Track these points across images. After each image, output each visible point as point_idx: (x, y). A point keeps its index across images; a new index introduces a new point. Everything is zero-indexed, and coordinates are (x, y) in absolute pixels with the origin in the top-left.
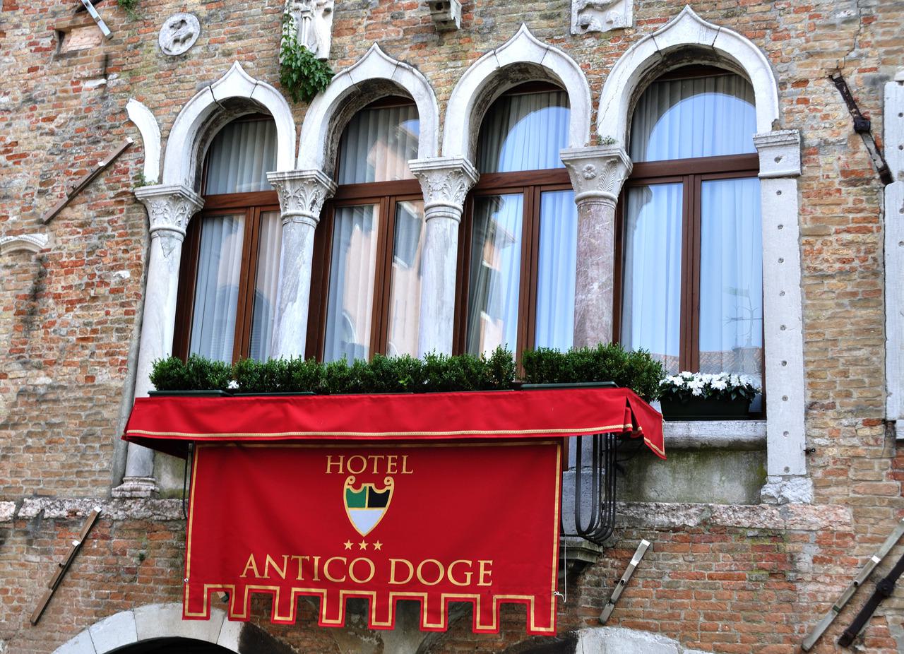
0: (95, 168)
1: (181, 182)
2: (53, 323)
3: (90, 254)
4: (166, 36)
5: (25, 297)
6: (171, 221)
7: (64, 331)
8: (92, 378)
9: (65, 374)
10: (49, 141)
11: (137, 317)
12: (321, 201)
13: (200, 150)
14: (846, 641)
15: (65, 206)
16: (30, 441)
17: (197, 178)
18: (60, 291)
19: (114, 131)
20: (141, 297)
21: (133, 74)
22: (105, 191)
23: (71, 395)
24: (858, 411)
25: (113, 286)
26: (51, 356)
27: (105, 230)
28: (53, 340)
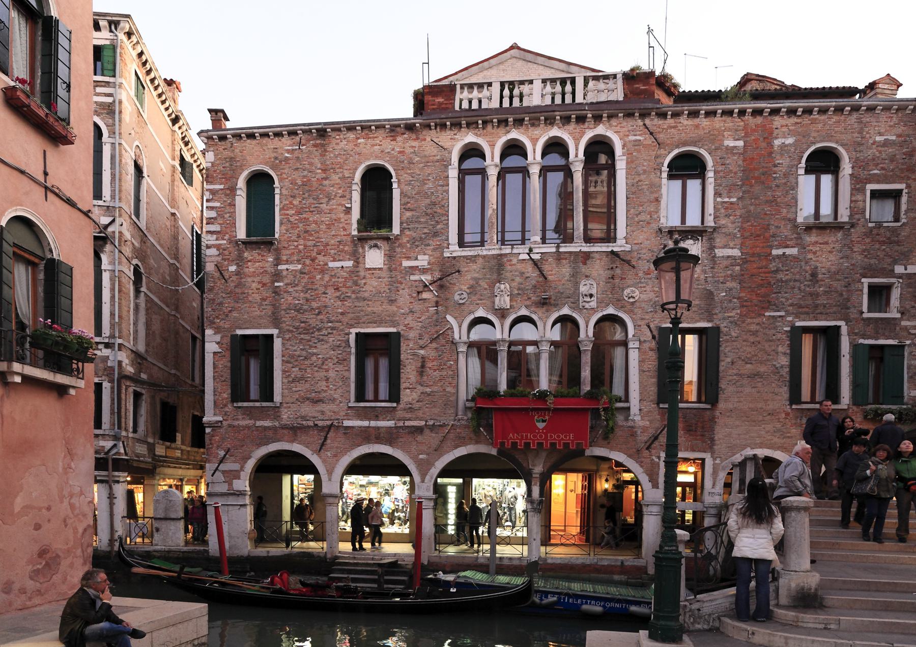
4: (457, 297)
9: (435, 388)
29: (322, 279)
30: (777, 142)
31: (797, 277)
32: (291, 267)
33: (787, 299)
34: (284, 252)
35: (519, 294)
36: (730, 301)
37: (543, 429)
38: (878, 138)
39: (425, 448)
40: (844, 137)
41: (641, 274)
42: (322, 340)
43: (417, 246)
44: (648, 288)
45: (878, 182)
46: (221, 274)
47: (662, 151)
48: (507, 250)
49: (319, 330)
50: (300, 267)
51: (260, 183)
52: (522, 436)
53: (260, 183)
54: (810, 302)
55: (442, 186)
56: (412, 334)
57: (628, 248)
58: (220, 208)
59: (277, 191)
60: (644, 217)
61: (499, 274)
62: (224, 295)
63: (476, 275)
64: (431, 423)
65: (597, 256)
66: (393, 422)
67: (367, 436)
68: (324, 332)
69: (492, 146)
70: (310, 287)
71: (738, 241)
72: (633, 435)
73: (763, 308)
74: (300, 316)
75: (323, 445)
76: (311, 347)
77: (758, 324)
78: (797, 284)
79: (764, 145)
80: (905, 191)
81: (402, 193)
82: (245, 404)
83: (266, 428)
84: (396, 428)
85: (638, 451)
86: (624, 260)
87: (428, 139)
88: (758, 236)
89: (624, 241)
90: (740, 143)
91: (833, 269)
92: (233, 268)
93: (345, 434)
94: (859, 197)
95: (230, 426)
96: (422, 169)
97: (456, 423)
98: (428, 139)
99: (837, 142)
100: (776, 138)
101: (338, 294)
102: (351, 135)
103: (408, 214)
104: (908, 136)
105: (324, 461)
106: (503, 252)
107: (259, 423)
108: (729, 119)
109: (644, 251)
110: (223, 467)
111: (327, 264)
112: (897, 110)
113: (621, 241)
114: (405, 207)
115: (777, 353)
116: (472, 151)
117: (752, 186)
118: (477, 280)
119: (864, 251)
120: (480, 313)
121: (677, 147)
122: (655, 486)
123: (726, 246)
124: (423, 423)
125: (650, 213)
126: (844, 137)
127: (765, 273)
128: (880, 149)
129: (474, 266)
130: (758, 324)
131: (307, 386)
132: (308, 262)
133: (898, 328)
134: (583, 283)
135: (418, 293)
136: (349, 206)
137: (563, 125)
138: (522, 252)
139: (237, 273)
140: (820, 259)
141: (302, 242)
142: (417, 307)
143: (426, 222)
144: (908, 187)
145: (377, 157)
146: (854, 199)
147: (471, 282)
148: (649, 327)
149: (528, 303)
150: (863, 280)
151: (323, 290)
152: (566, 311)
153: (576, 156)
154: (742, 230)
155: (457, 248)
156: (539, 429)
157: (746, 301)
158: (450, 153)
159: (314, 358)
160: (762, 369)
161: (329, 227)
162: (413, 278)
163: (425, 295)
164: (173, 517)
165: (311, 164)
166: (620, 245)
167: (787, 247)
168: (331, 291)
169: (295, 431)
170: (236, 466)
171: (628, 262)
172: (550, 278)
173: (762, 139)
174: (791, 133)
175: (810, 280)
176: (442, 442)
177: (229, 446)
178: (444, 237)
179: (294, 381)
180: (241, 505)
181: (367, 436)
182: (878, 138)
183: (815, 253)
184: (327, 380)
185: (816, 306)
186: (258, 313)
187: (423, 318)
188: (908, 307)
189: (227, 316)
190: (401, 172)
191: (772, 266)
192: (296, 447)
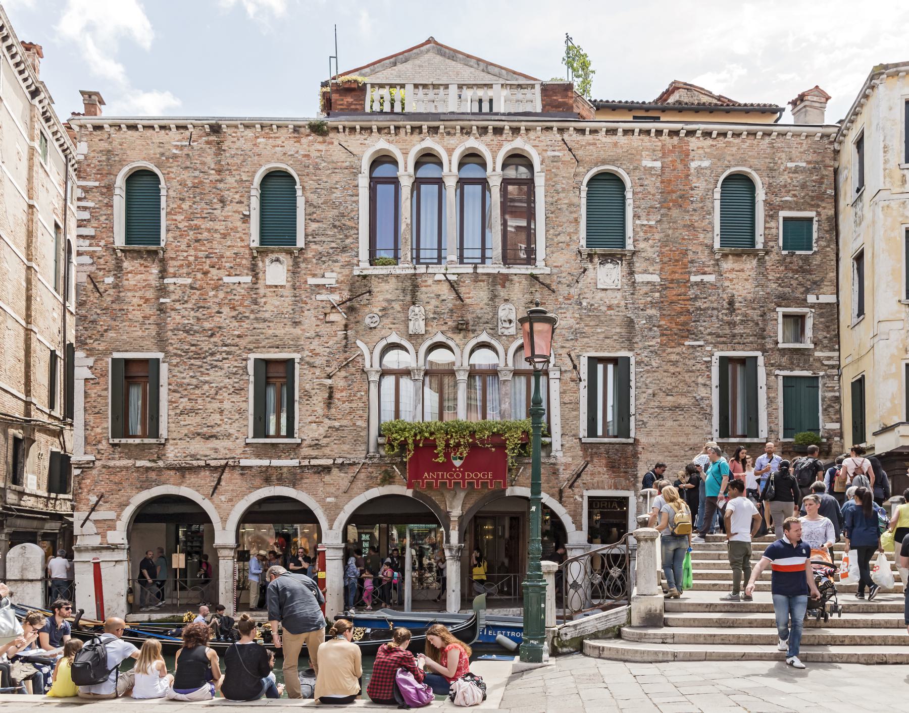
4: (367, 321)
6: (374, 377)
10: (328, 350)
14: (570, 487)
21: (357, 332)
24: (574, 436)
29: (215, 296)
30: (693, 165)
31: (715, 305)
32: (180, 281)
33: (706, 328)
34: (171, 263)
35: (434, 318)
36: (650, 329)
37: (460, 467)
38: (790, 165)
39: (332, 490)
40: (756, 162)
41: (561, 299)
42: (216, 366)
43: (324, 262)
44: (568, 315)
45: (791, 209)
46: (95, 286)
47: (581, 169)
48: (421, 269)
49: (212, 354)
50: (189, 281)
51: (142, 183)
52: (438, 475)
53: (142, 183)
54: (728, 331)
55: (352, 196)
57: (547, 271)
58: (94, 208)
59: (163, 192)
60: (562, 238)
61: (414, 296)
62: (99, 311)
63: (389, 297)
64: (339, 461)
65: (516, 278)
66: (297, 461)
67: (268, 476)
68: (218, 357)
69: (406, 154)
70: (201, 304)
71: (658, 267)
72: (555, 473)
73: (682, 337)
74: (189, 338)
75: (215, 488)
76: (202, 374)
77: (678, 354)
78: (715, 312)
79: (680, 167)
80: (816, 219)
81: (307, 202)
82: (124, 441)
83: (148, 469)
84: (301, 467)
85: (561, 492)
86: (543, 284)
87: (336, 143)
88: (677, 261)
89: (544, 263)
90: (658, 164)
91: (749, 297)
92: (110, 280)
93: (242, 474)
94: (773, 224)
95: (104, 467)
96: (329, 176)
97: (367, 461)
98: (336, 143)
99: (751, 167)
100: (693, 160)
101: (234, 313)
102: (249, 133)
103: (314, 226)
104: (817, 163)
105: (217, 507)
106: (418, 272)
107: (139, 463)
108: (646, 138)
109: (564, 275)
110: (94, 516)
111: (221, 279)
112: (807, 137)
113: (540, 263)
114: (310, 218)
115: (697, 384)
116: (382, 159)
117: (669, 209)
118: (389, 301)
119: (778, 279)
120: (394, 338)
121: (596, 165)
122: (579, 528)
123: (645, 272)
124: (330, 462)
125: (569, 234)
126: (756, 162)
127: (684, 300)
128: (791, 175)
129: (384, 286)
130: (678, 354)
131: (198, 419)
132: (199, 275)
133: (811, 359)
134: (502, 307)
135: (326, 314)
136: (247, 213)
137: (480, 135)
138: (438, 271)
139: (116, 286)
140: (737, 286)
141: (192, 252)
142: (324, 329)
143: (334, 236)
144: (818, 214)
145: (279, 161)
146: (767, 225)
147: (385, 304)
148: (570, 355)
149: (444, 328)
150: (778, 309)
151: (217, 309)
152: (484, 337)
153: (494, 170)
154: (661, 254)
155: (367, 265)
156: (456, 468)
157: (666, 329)
158: (360, 159)
159: (206, 387)
160: (683, 401)
161: (224, 236)
162: (319, 297)
163: (333, 317)
164: (31, 578)
165: (203, 163)
166: (540, 268)
167: (704, 273)
168: (226, 310)
169: (183, 471)
170: (111, 515)
171: (548, 287)
172: (467, 301)
173: (679, 161)
174: (707, 156)
175: (728, 309)
176: (352, 482)
177: (103, 490)
178: (354, 253)
179: (181, 413)
180: (116, 561)
181: (268, 476)
182: (790, 165)
183: (731, 280)
184: (221, 412)
185: (734, 336)
186: (140, 333)
187: (331, 343)
188: (820, 337)
189: (102, 335)
190: (306, 179)
191: (691, 293)
192: (184, 491)
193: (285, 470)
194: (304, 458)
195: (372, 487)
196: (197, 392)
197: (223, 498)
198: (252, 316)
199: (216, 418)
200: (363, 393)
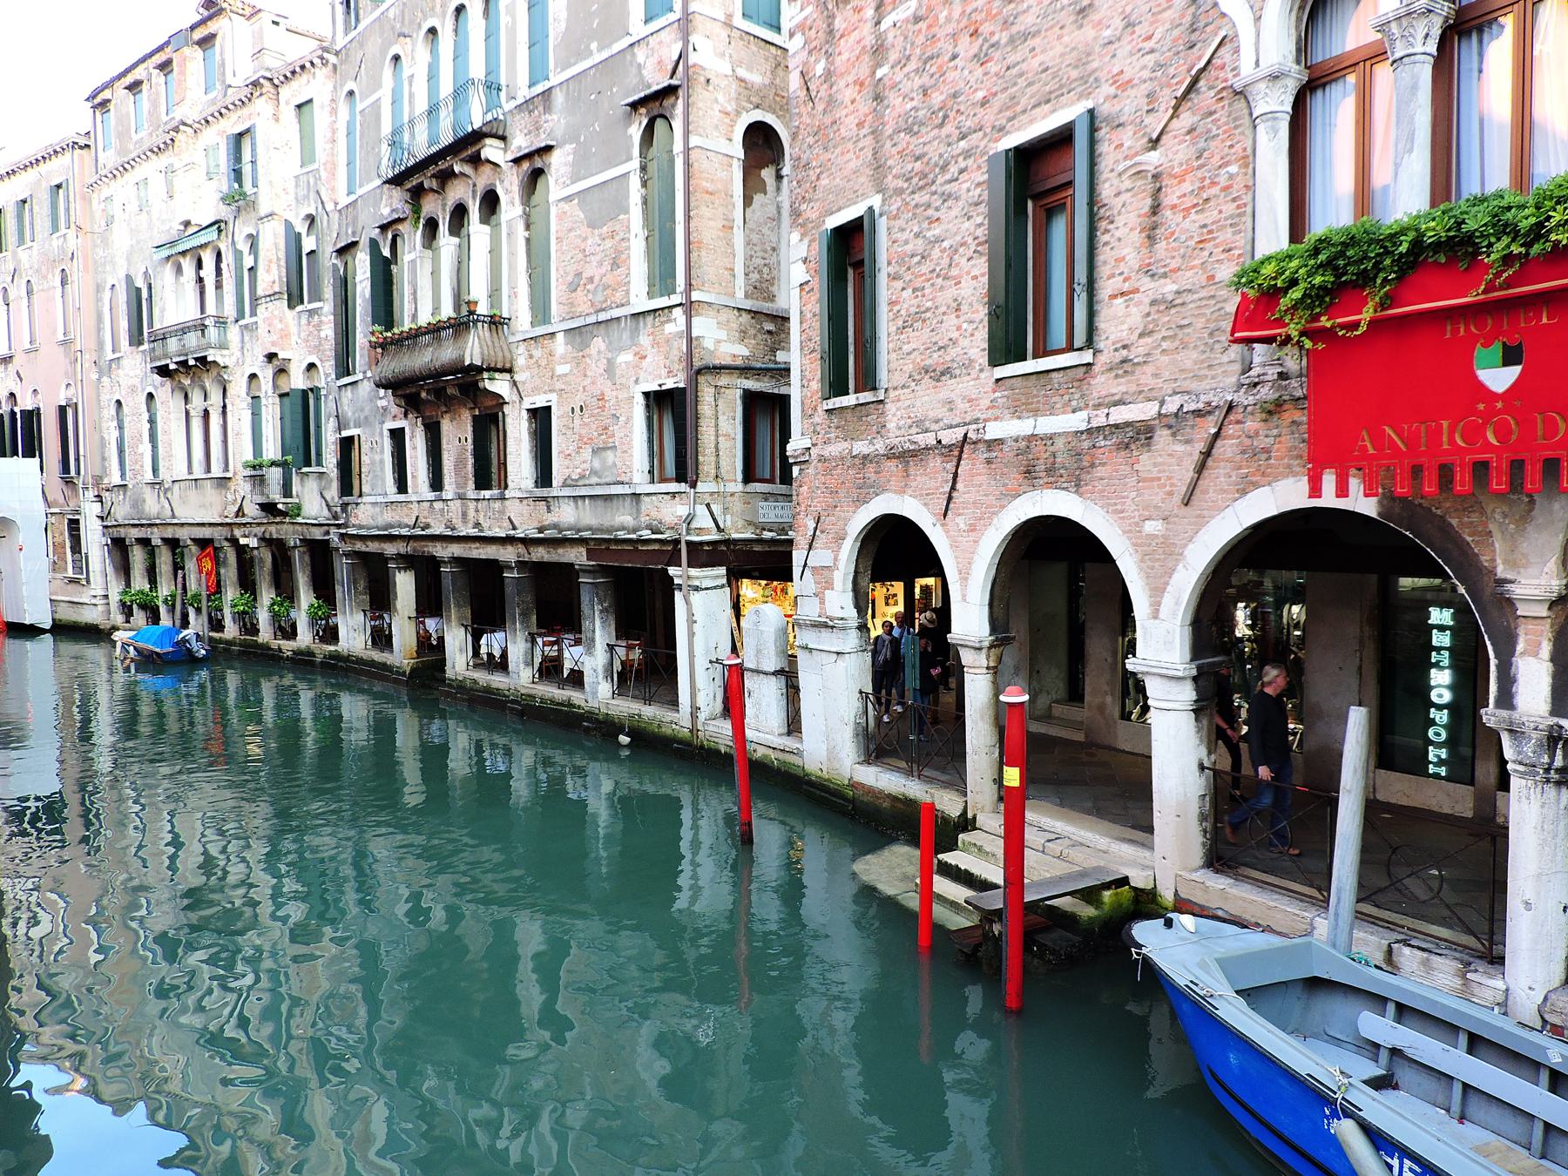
0: (1193, 72)
1: (1281, 60)
2: (1173, 233)
3: (1198, 158)
5: (1145, 215)
7: (1183, 238)
8: (1213, 277)
9: (1188, 278)
11: (1249, 209)
12: (1436, 32)
13: (1299, 19)
15: (1172, 118)
16: (1165, 345)
17: (1298, 50)
18: (1176, 201)
19: (1208, 29)
20: (1251, 188)
22: (1206, 95)
23: (1196, 296)
25: (1223, 184)
26: (1174, 264)
27: (1209, 131)
28: (1174, 249)
49: (944, 168)
56: (1130, 104)
64: (1171, 406)
66: (1083, 415)
67: (1034, 462)
68: (953, 169)
105: (954, 545)
176: (1201, 468)
181: (1034, 462)
193: (1060, 443)
194: (1098, 406)
195: (1256, 485)
196: (924, 269)
197: (960, 521)
198: (1004, 37)
199: (951, 320)
200: (1233, 169)
